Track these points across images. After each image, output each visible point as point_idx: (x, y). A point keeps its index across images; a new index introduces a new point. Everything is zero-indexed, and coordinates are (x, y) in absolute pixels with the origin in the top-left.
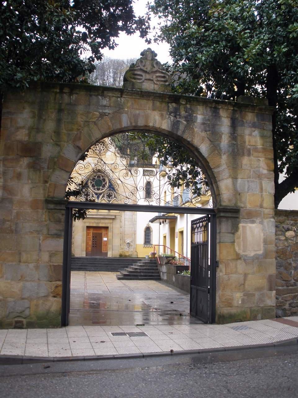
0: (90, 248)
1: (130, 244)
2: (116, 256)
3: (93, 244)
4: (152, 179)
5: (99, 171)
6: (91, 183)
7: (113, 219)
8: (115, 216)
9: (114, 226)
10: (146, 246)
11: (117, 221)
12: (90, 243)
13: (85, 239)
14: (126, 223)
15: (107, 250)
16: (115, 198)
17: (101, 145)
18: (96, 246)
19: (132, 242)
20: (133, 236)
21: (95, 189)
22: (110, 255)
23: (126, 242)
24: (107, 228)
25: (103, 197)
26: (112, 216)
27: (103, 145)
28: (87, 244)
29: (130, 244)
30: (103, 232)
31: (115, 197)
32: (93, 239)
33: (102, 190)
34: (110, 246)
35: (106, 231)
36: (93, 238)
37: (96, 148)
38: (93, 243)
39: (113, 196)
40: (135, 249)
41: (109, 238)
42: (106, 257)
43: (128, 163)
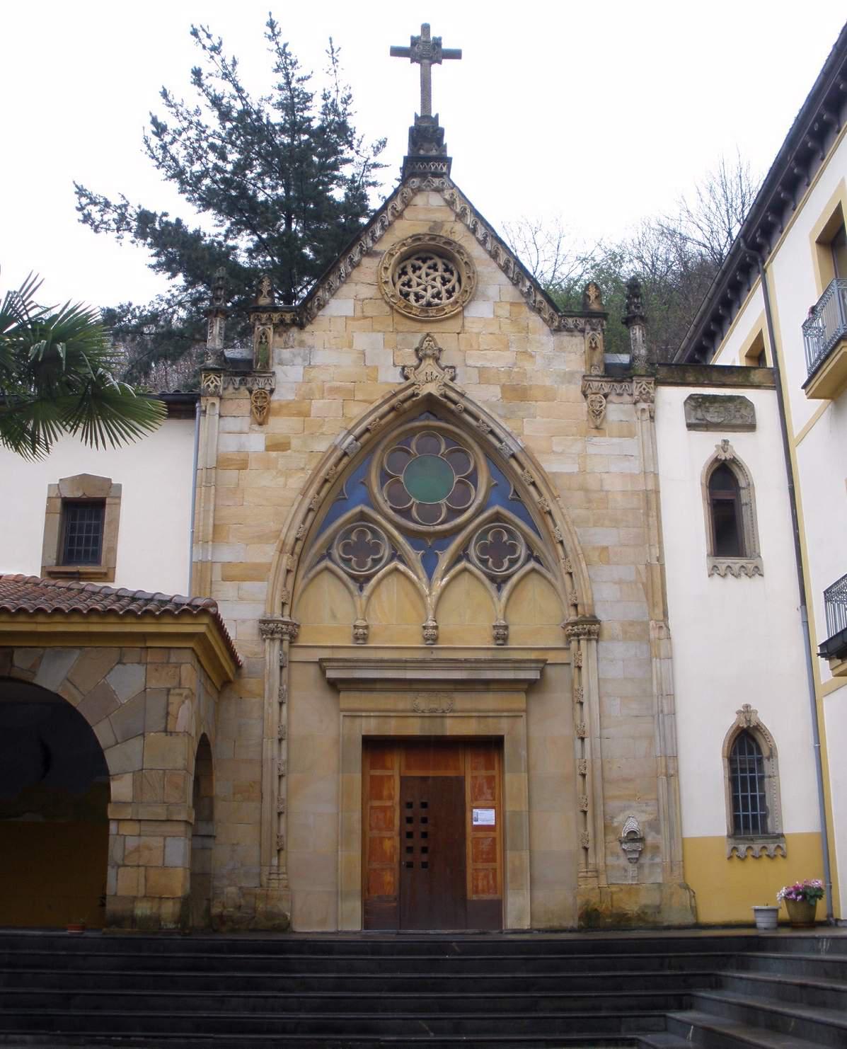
1: (642, 840)
2: (556, 924)
3: (410, 850)
4: (741, 446)
5: (432, 405)
6: (384, 477)
7: (531, 687)
8: (542, 665)
10: (742, 848)
11: (557, 698)
12: (391, 843)
13: (357, 816)
14: (615, 708)
15: (498, 886)
16: (532, 564)
17: (434, 268)
18: (425, 865)
19: (654, 825)
20: (662, 790)
21: (406, 513)
22: (519, 913)
23: (616, 830)
24: (490, 746)
25: (461, 555)
26: (518, 664)
27: (447, 270)
28: (370, 850)
29: (642, 840)
30: (470, 770)
31: (530, 557)
32: (409, 820)
33: (454, 513)
34: (515, 859)
35: (489, 766)
36: (409, 813)
37: (408, 284)
38: (410, 843)
39: (522, 551)
40: (677, 872)
41: (509, 807)
42: (494, 935)
43: (597, 357)
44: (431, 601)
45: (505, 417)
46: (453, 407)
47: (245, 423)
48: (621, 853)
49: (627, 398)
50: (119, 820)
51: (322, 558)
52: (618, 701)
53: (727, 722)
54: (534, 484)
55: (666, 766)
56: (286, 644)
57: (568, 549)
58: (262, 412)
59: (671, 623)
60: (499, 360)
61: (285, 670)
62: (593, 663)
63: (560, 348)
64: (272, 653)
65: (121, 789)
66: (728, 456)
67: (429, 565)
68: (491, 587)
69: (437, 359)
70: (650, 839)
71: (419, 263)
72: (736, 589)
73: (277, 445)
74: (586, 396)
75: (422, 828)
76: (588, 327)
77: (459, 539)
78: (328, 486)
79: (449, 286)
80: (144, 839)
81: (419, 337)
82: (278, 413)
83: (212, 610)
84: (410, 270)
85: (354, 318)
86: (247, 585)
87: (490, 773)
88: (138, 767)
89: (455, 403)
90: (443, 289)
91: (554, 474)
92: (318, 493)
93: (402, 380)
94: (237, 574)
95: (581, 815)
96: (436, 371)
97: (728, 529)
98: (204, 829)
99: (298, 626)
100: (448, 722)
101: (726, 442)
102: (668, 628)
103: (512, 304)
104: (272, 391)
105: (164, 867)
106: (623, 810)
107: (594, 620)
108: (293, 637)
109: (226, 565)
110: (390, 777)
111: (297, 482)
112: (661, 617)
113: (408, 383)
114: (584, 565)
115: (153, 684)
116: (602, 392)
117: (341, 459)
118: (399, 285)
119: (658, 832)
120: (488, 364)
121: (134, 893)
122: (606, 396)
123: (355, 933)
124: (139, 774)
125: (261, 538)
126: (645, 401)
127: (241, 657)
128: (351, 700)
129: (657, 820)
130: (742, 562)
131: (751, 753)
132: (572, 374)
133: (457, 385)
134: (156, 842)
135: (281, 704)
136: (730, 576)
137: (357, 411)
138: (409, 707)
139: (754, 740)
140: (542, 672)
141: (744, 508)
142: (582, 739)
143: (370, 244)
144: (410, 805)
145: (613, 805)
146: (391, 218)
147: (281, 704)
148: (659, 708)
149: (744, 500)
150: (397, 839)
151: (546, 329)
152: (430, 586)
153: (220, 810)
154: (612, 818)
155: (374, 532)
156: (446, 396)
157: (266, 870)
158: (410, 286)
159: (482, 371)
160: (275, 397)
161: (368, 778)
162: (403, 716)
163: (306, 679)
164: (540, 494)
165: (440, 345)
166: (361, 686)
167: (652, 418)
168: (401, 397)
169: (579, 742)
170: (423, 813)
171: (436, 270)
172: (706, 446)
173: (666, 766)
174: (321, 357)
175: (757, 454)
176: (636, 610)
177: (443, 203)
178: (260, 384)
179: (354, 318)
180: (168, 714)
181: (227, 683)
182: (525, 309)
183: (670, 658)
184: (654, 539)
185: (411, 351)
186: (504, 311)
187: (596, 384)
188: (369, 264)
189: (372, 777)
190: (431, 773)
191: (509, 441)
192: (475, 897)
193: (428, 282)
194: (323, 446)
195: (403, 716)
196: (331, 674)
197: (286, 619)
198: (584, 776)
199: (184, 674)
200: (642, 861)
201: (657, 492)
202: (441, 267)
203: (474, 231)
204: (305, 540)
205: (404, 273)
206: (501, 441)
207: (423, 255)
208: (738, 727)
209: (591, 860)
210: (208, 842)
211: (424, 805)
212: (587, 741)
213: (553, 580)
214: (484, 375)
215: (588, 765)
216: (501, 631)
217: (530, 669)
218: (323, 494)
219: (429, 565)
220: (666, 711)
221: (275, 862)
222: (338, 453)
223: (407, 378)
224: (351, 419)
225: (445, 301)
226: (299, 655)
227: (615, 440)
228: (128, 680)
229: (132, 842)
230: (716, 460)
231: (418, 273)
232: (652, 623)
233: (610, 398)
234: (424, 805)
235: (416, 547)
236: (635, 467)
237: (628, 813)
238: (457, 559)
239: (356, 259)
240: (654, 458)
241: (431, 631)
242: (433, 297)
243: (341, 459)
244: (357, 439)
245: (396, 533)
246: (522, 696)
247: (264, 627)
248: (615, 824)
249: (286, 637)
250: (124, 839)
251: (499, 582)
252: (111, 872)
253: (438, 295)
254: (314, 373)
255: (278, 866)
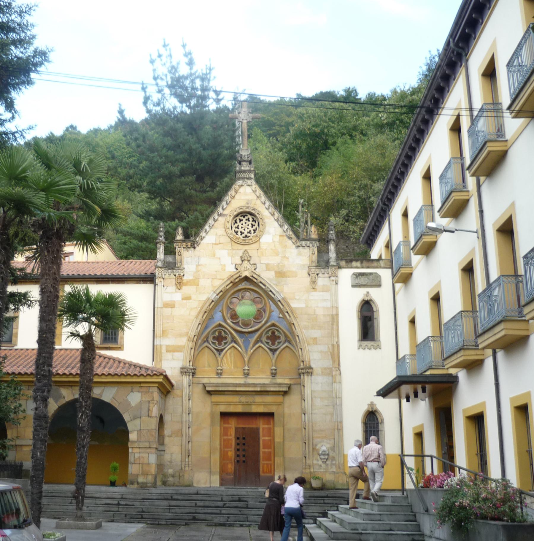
0: (231, 467)
1: (328, 455)
3: (238, 456)
4: (374, 294)
7: (285, 393)
9: (287, 411)
12: (231, 453)
13: (218, 443)
14: (318, 402)
17: (248, 220)
18: (244, 461)
19: (333, 449)
21: (237, 324)
23: (318, 450)
27: (254, 220)
28: (223, 457)
30: (262, 425)
35: (269, 424)
36: (238, 441)
38: (238, 453)
39: (283, 339)
44: (246, 359)
45: (276, 285)
46: (255, 281)
47: (172, 288)
48: (319, 459)
49: (326, 275)
50: (132, 448)
51: (205, 342)
52: (319, 399)
53: (363, 409)
54: (287, 312)
55: (338, 426)
56: (191, 377)
57: (300, 339)
58: (180, 283)
59: (341, 368)
60: (274, 261)
61: (191, 387)
62: (309, 384)
63: (299, 254)
64: (186, 380)
65: (133, 436)
66: (368, 298)
67: (246, 343)
68: (270, 353)
69: (249, 261)
70: (331, 454)
71: (242, 218)
72: (368, 354)
73: (187, 298)
74: (309, 275)
75: (243, 447)
76: (311, 245)
77: (259, 332)
78: (206, 314)
79: (254, 228)
80: (141, 455)
81: (242, 251)
82: (187, 284)
83: (164, 374)
84: (238, 221)
85: (216, 244)
86: (176, 354)
87: (269, 426)
88: (139, 428)
89: (256, 279)
90: (252, 229)
91: (296, 308)
92: (202, 317)
93: (235, 270)
94: (171, 350)
95: (304, 444)
96: (249, 266)
97: (368, 330)
98: (161, 448)
99: (195, 369)
100: (253, 407)
101: (368, 292)
102: (340, 370)
103: (280, 236)
104: (184, 275)
105: (148, 464)
106: (320, 442)
107: (311, 368)
108: (194, 374)
109: (167, 346)
110: (231, 428)
111: (194, 313)
112: (337, 366)
113: (238, 271)
114: (306, 345)
115: (143, 399)
116: (316, 273)
117: (211, 303)
118: (234, 228)
119: (334, 451)
120: (270, 262)
121: (138, 473)
122: (317, 274)
123: (217, 487)
124: (139, 431)
125: (181, 335)
126: (334, 276)
127: (173, 382)
128: (216, 398)
129: (334, 446)
130: (372, 343)
131: (374, 421)
132: (304, 265)
133: (258, 271)
134: (145, 455)
135: (189, 400)
136: (367, 349)
137: (218, 283)
138: (238, 400)
139: (375, 415)
140: (289, 388)
141: (375, 320)
142: (305, 414)
143: (221, 211)
144: (238, 438)
145: (316, 441)
146: (230, 199)
147: (189, 400)
148: (335, 402)
149: (375, 317)
150: (234, 451)
151: (294, 246)
152: (247, 355)
153: (167, 440)
154: (316, 445)
155: (224, 331)
156: (252, 276)
157: (183, 463)
158: (238, 228)
159: (267, 265)
160: (185, 278)
161: (222, 428)
162: (235, 404)
163: (198, 389)
164: (290, 317)
165: (250, 255)
166: (219, 393)
167: (337, 283)
168: (235, 277)
169: (303, 415)
170: (243, 441)
171: (249, 221)
172: (360, 294)
173: (338, 426)
174: (203, 261)
175: (381, 298)
176: (328, 363)
177: (252, 191)
178: (178, 273)
179: (216, 244)
180: (149, 410)
181: (168, 392)
182: (285, 238)
183: (340, 383)
184: (335, 335)
185: (239, 258)
186: (277, 239)
187: (313, 270)
188: (221, 220)
189: (224, 428)
190: (247, 426)
191: (277, 295)
192: (263, 474)
193: (246, 225)
194: (204, 298)
195: (235, 404)
196: (208, 389)
197: (191, 367)
198: (305, 429)
199: (154, 396)
200: (328, 462)
201: (337, 315)
202: (251, 219)
203: (264, 203)
204: (199, 335)
205: (236, 222)
206: (274, 295)
207: (244, 214)
208: (368, 411)
209: (307, 462)
210: (162, 453)
211: (244, 438)
212: (306, 415)
213: (294, 350)
214: (268, 267)
215: (307, 424)
216: (274, 371)
217: (284, 387)
218: (204, 317)
219: (246, 343)
220: (338, 404)
221: (187, 460)
222: (211, 301)
223: (237, 269)
224: (215, 287)
225: (253, 234)
226: (195, 380)
227: (321, 293)
228: (135, 398)
229: (137, 456)
230: (364, 300)
231: (242, 222)
232: (334, 369)
233: (319, 275)
234: (244, 438)
235: (240, 337)
236: (329, 304)
237: (322, 443)
238: (257, 342)
239: (216, 218)
240: (337, 301)
241: (246, 371)
242: (248, 233)
243: (211, 303)
244: (217, 295)
245: (233, 332)
246: (281, 397)
247: (182, 370)
248: (317, 448)
249: (191, 374)
250: (134, 454)
251: (273, 351)
252: (130, 466)
253: (250, 232)
254: (200, 268)
255: (188, 462)
